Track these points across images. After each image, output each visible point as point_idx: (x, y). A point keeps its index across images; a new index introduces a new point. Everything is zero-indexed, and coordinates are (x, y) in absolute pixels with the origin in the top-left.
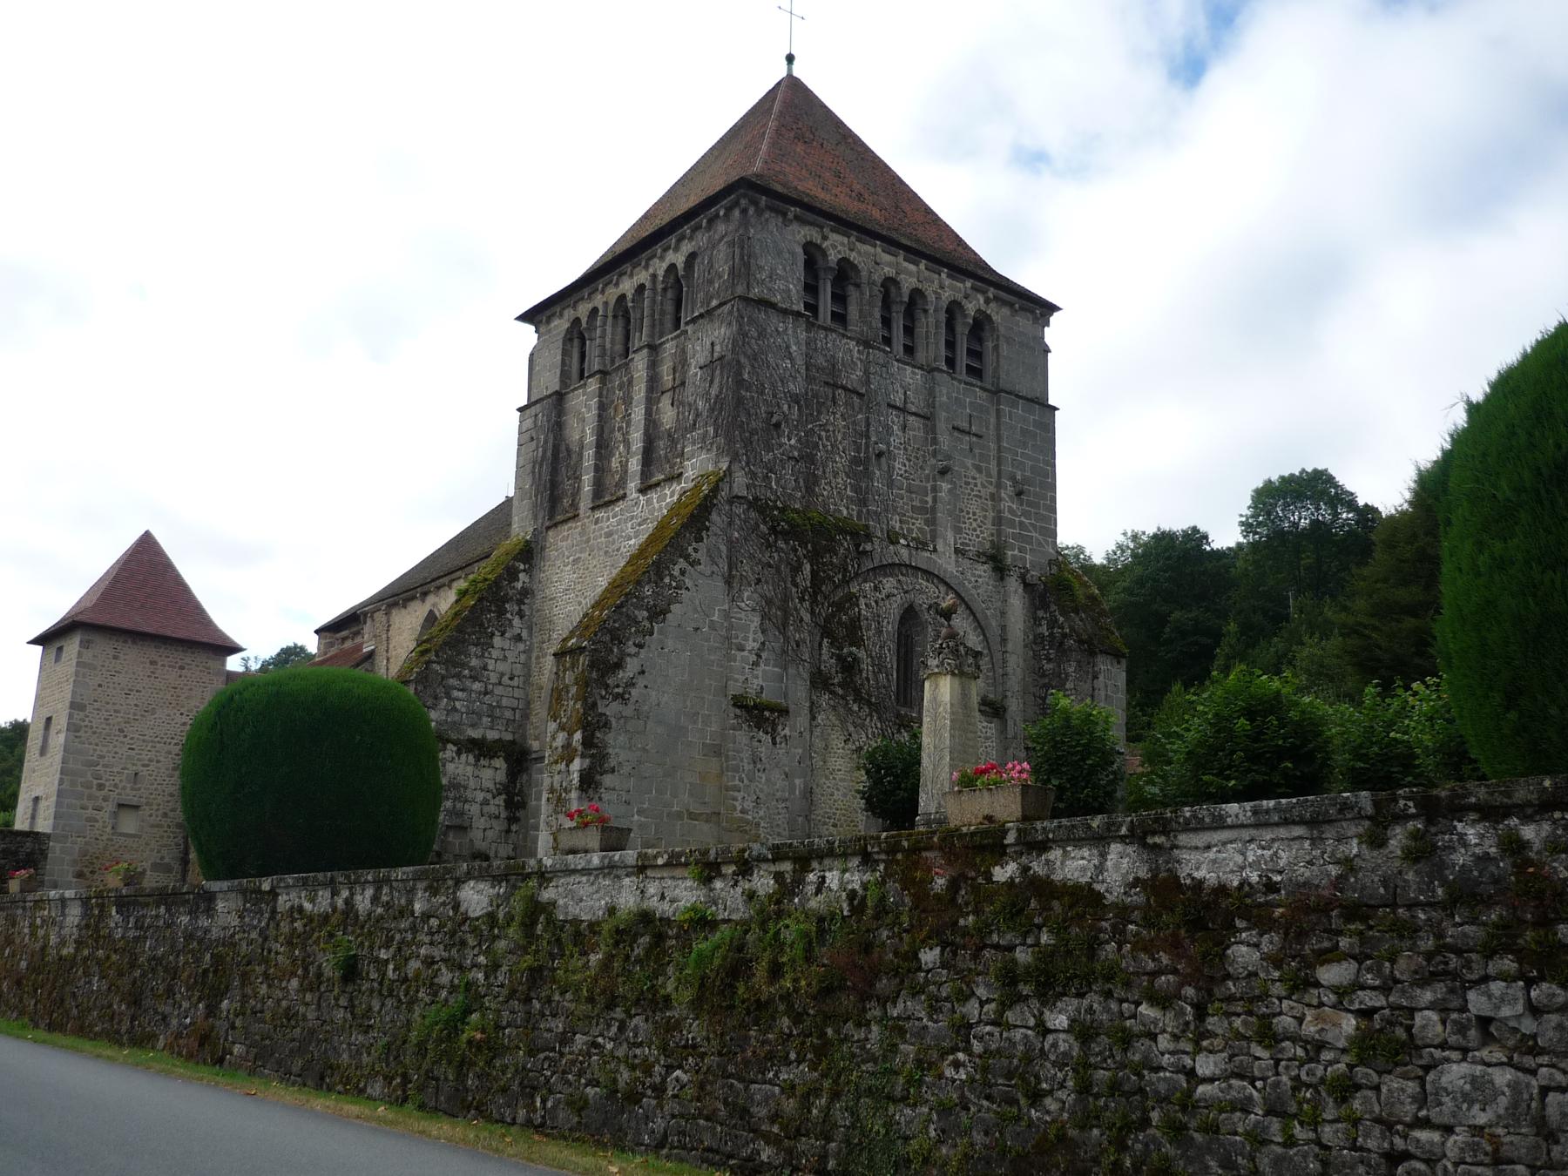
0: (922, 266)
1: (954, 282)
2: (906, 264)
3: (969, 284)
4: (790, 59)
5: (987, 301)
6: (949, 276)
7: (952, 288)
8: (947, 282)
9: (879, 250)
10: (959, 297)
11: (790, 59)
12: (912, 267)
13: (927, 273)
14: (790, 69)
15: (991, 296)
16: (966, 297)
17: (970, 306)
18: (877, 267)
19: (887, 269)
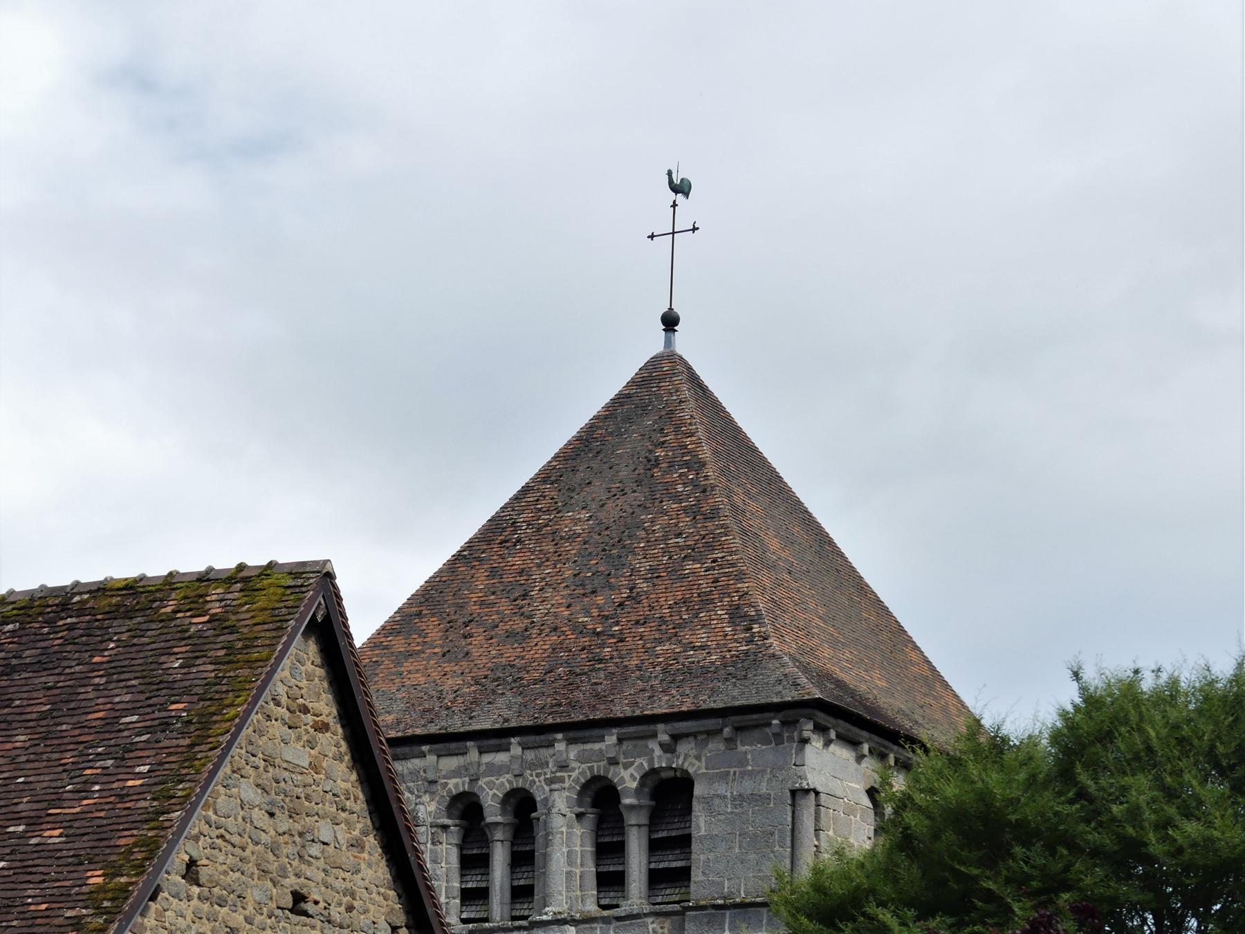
0: (516, 750)
1: (589, 746)
2: (487, 758)
3: (611, 739)
4: (670, 322)
5: (668, 749)
6: (571, 741)
7: (581, 759)
8: (573, 752)
9: (431, 759)
10: (599, 767)
11: (670, 322)
12: (501, 758)
13: (530, 755)
14: (668, 343)
15: (664, 738)
16: (613, 762)
17: (625, 774)
18: (434, 788)
19: (452, 783)
